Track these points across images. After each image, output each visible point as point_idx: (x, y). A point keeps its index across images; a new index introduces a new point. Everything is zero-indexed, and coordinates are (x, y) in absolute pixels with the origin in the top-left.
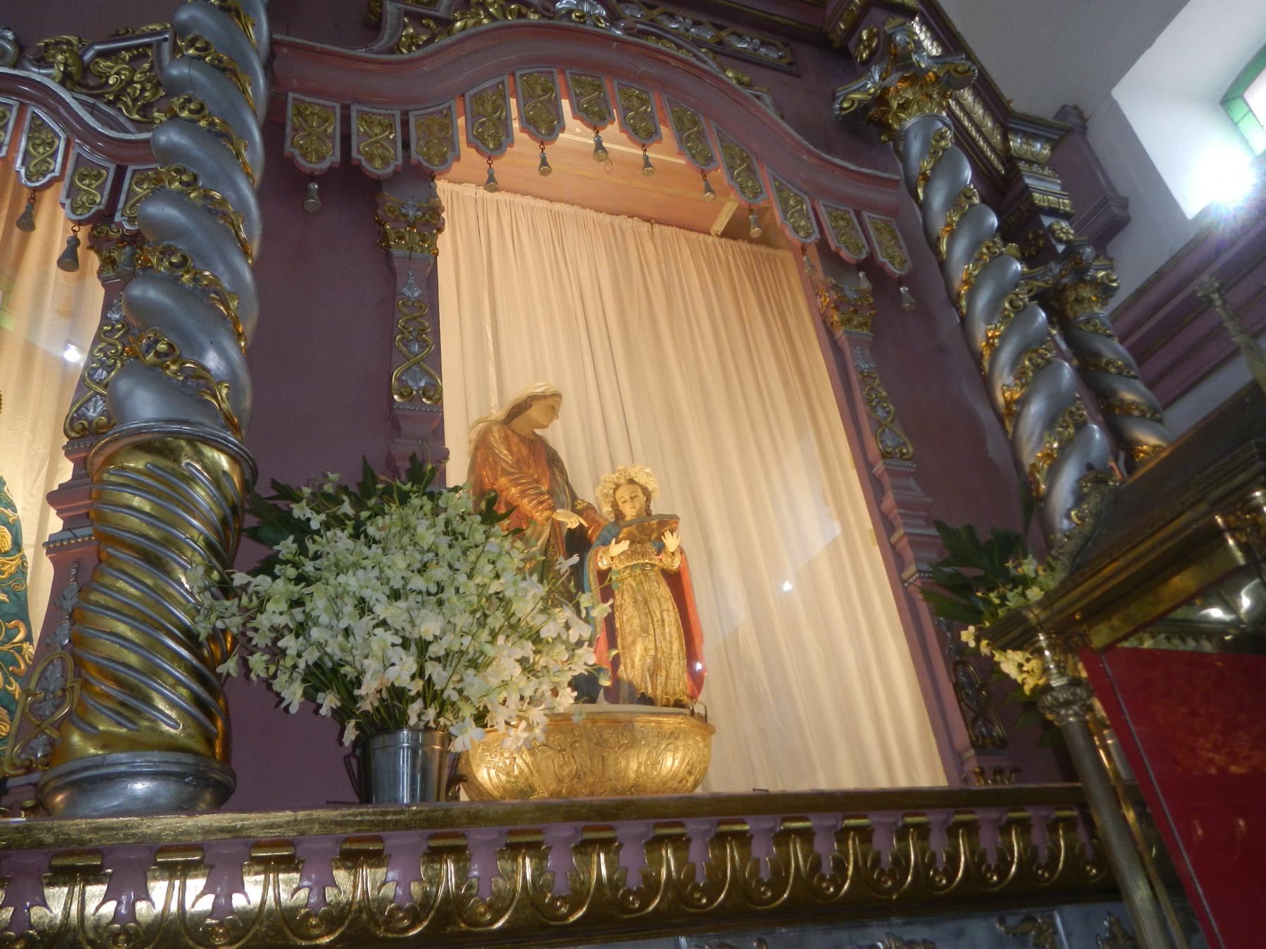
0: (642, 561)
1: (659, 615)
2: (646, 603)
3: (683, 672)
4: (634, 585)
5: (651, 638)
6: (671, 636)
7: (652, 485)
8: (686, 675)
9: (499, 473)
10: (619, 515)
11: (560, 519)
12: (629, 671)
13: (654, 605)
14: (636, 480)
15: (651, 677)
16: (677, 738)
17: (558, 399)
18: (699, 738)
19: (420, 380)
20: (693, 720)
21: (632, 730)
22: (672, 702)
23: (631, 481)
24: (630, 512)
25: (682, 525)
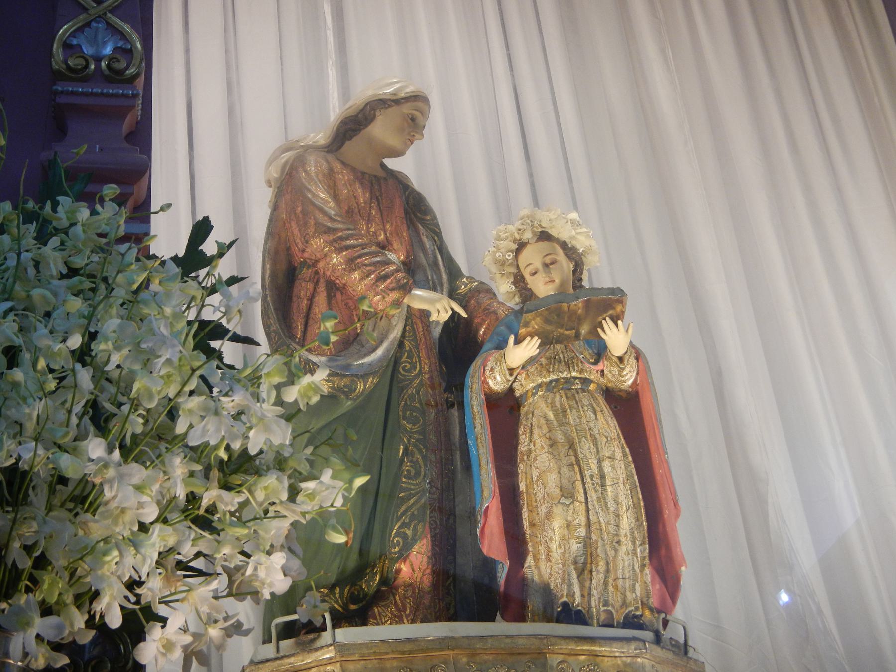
0: (566, 375)
1: (594, 467)
2: (572, 446)
3: (643, 566)
4: (551, 415)
6: (617, 502)
7: (581, 243)
8: (647, 571)
9: (311, 231)
11: (417, 305)
12: (542, 565)
13: (586, 448)
14: (553, 233)
15: (580, 574)
17: (420, 104)
19: (105, 44)
20: (658, 651)
22: (619, 617)
23: (544, 236)
24: (542, 287)
25: (631, 308)
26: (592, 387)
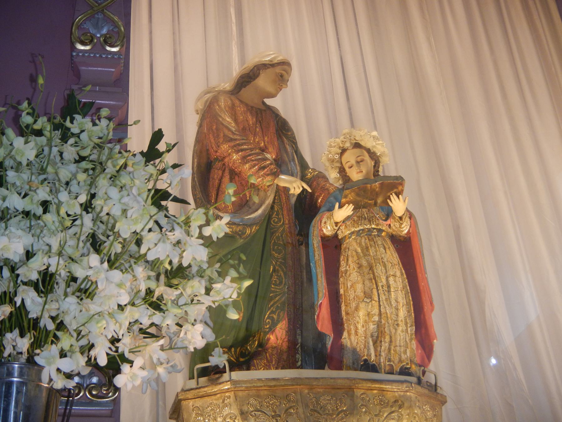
0: (368, 226)
1: (384, 281)
2: (371, 268)
3: (411, 340)
4: (359, 250)
5: (377, 304)
6: (397, 301)
7: (379, 149)
8: (414, 342)
9: (221, 140)
10: (346, 178)
11: (282, 184)
12: (353, 337)
13: (379, 270)
14: (362, 143)
15: (375, 343)
16: (400, 407)
17: (286, 67)
18: (427, 408)
19: (102, 27)
20: (419, 389)
21: (352, 397)
22: (397, 369)
23: (357, 145)
24: (355, 175)
25: (407, 188)
26: (383, 234)
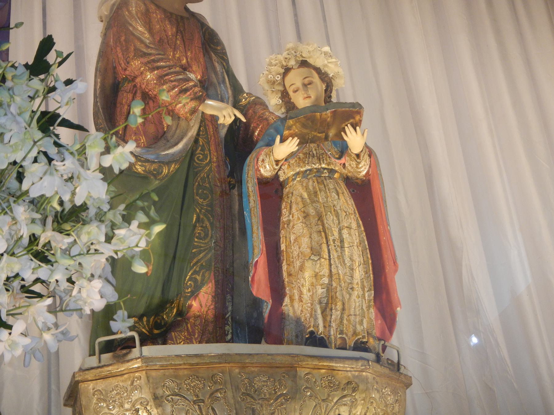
0: (317, 166)
1: (336, 234)
2: (320, 218)
3: (369, 307)
4: (305, 195)
5: (326, 263)
6: (351, 259)
8: (372, 310)
9: (131, 55)
10: (289, 105)
11: (209, 112)
12: (296, 305)
13: (330, 220)
14: (311, 61)
15: (323, 312)
16: (354, 391)
18: (387, 391)
20: (378, 367)
21: (295, 376)
22: (351, 343)
23: (304, 64)
26: (336, 176)
